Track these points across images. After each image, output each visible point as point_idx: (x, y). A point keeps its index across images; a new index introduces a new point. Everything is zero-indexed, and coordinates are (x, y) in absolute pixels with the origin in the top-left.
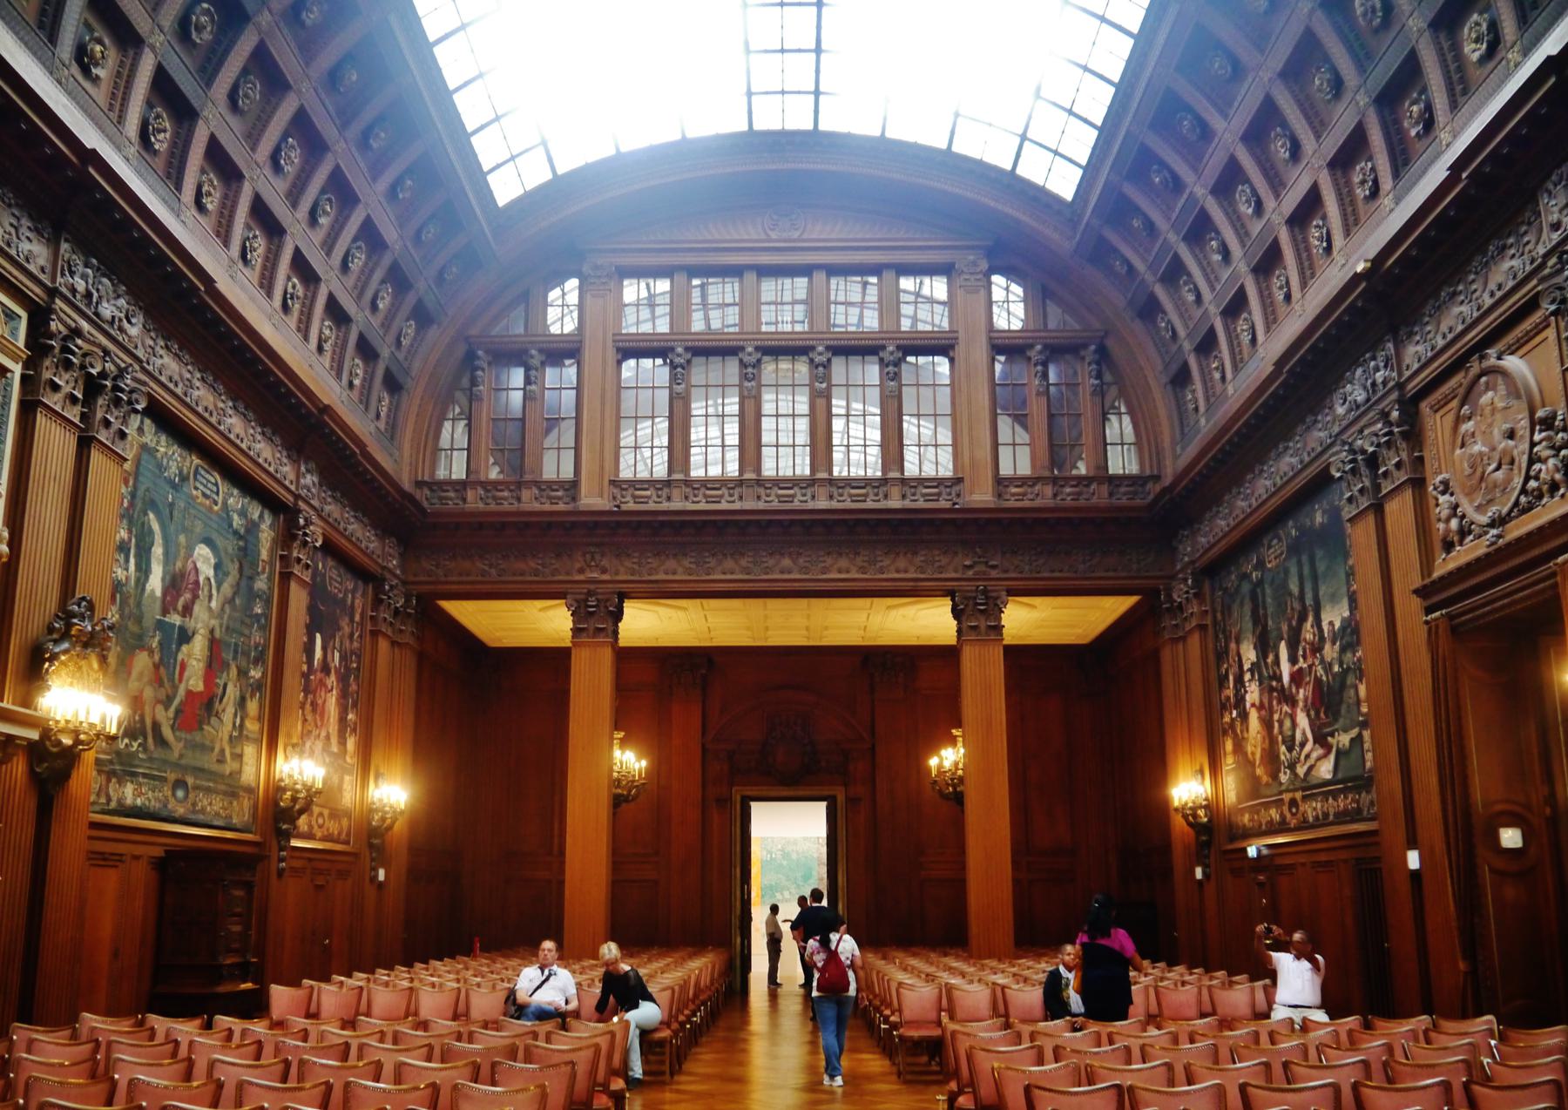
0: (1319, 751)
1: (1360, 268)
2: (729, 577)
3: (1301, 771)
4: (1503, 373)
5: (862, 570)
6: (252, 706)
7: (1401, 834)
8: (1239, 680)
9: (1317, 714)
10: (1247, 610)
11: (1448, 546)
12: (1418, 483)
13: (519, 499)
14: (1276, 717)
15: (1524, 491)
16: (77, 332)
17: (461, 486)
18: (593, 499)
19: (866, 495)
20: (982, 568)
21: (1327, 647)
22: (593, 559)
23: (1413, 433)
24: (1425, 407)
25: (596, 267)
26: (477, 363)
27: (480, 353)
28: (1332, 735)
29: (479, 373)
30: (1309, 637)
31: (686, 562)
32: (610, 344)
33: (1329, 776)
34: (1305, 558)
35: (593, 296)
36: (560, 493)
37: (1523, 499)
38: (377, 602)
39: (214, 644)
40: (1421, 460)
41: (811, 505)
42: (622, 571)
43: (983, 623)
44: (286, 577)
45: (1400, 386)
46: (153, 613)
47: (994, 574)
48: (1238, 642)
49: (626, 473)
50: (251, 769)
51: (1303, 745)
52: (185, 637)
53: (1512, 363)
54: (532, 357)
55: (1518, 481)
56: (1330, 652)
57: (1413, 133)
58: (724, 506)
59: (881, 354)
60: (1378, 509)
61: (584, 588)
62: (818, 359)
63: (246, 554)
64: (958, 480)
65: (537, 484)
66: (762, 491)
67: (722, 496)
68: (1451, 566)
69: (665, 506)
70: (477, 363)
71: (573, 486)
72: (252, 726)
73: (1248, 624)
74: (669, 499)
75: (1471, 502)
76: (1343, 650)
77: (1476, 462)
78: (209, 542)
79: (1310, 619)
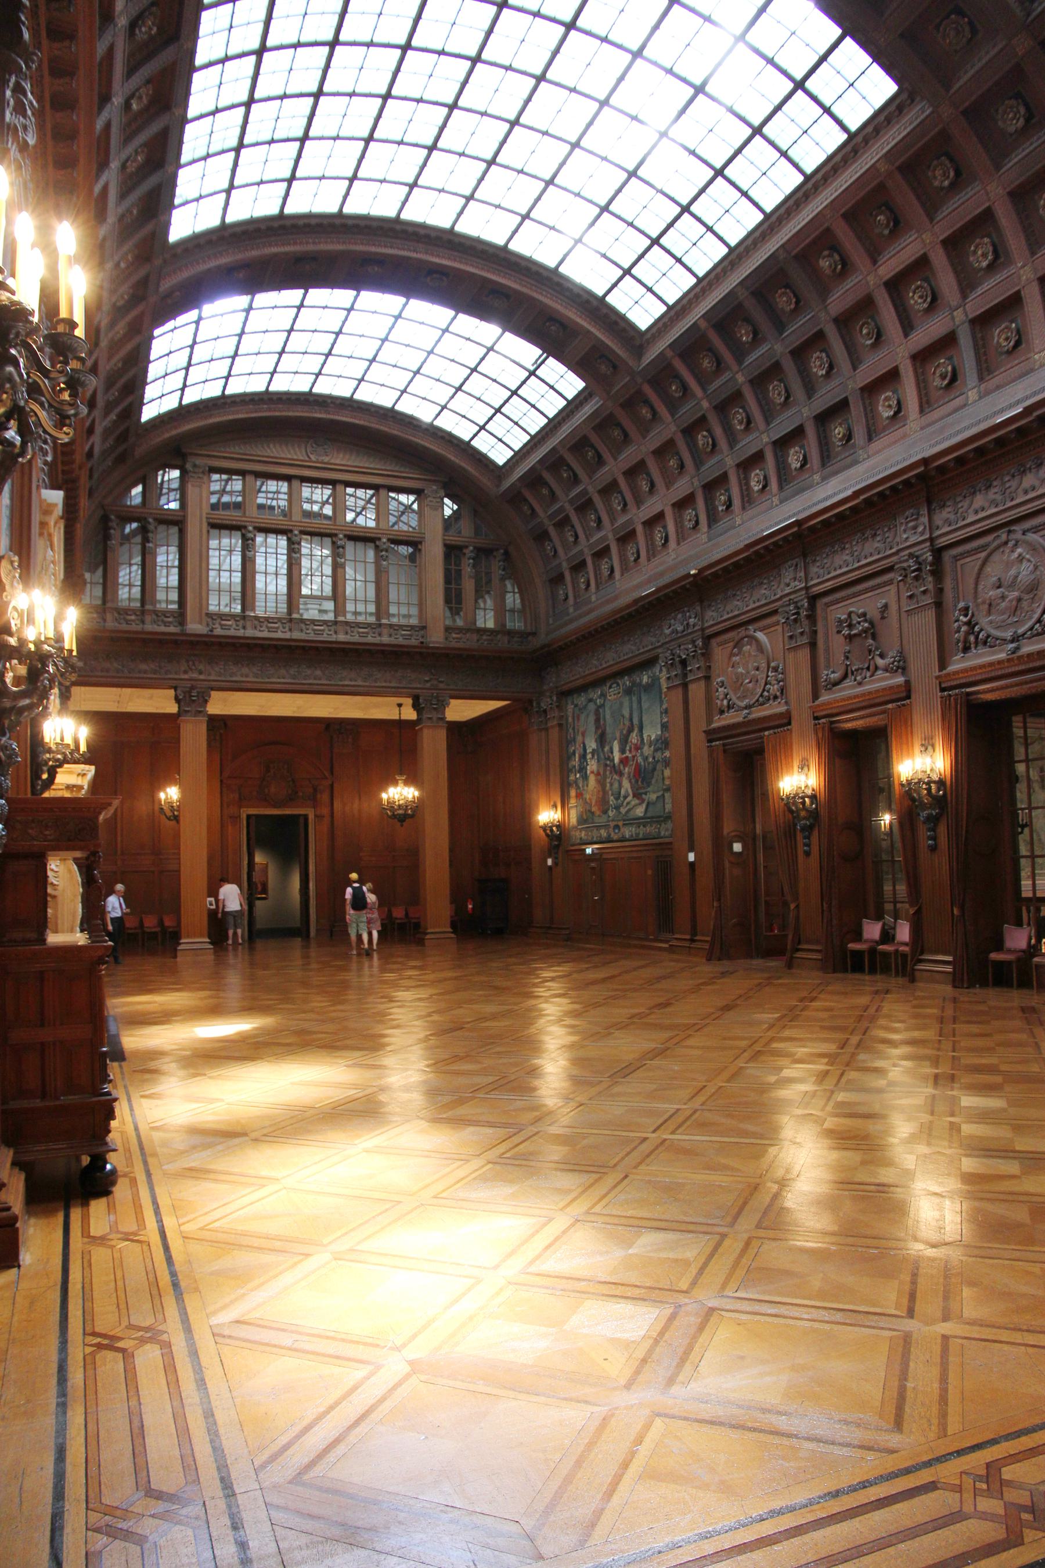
0: (636, 801)
1: (692, 572)
2: (282, 680)
3: (623, 810)
4: (757, 640)
5: (365, 679)
7: (686, 844)
8: (583, 756)
9: (637, 782)
10: (592, 719)
11: (722, 712)
12: (707, 678)
13: (143, 622)
14: (608, 780)
15: (761, 695)
18: (195, 627)
19: (367, 633)
20: (435, 682)
21: (646, 748)
22: (194, 664)
23: (707, 654)
24: (714, 642)
25: (195, 466)
26: (110, 524)
27: (113, 517)
28: (646, 794)
29: (112, 531)
30: (634, 741)
31: (255, 670)
32: (204, 520)
33: (641, 815)
34: (634, 698)
35: (193, 486)
36: (170, 619)
37: (761, 699)
40: (710, 667)
41: (333, 638)
42: (214, 673)
43: (435, 715)
45: (703, 630)
47: (441, 686)
48: (583, 735)
49: (213, 608)
51: (625, 797)
53: (759, 635)
54: (149, 523)
55: (759, 691)
56: (647, 751)
57: (720, 509)
58: (279, 635)
59: (378, 543)
60: (685, 686)
61: (188, 684)
62: (339, 543)
64: (424, 628)
65: (156, 612)
66: (303, 626)
67: (278, 628)
68: (723, 723)
69: (241, 633)
70: (110, 524)
71: (181, 615)
73: (592, 727)
74: (244, 628)
75: (735, 694)
76: (656, 750)
77: (739, 677)
79: (636, 731)
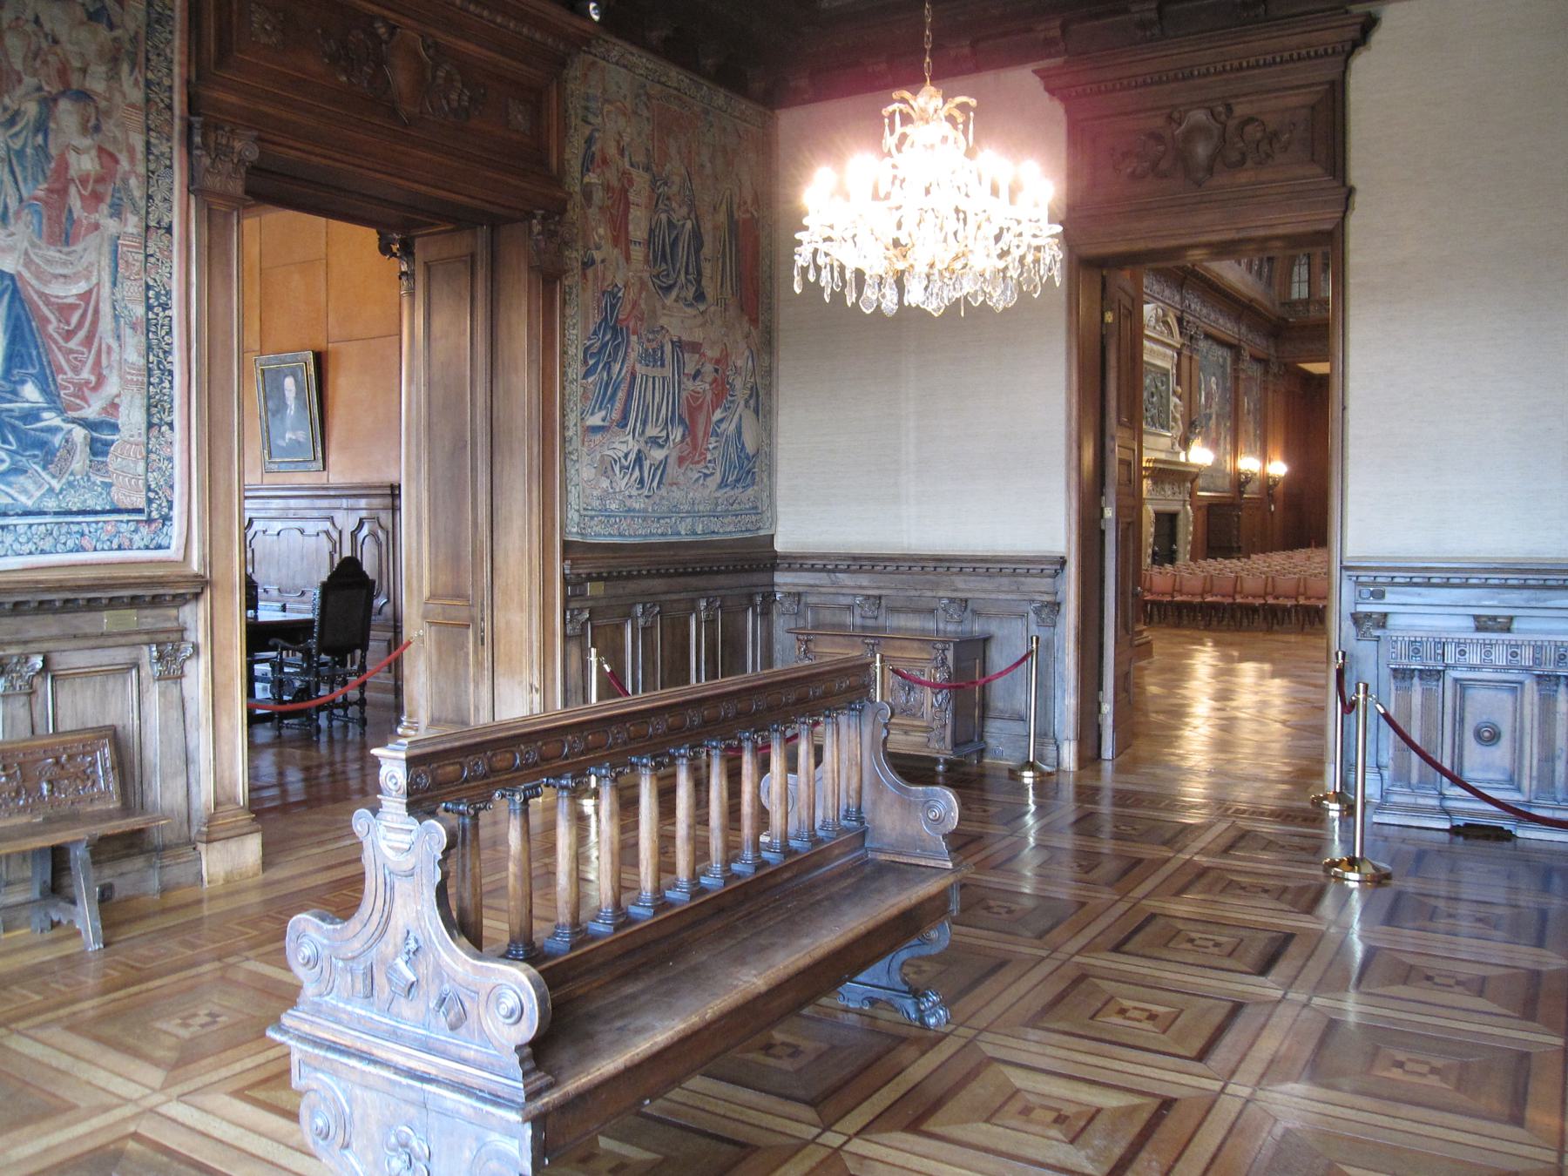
6: (1228, 438)
16: (1188, 322)
17: (1307, 302)
38: (1266, 372)
39: (1218, 416)
44: (1237, 378)
46: (1203, 412)
50: (1229, 466)
52: (1210, 418)
63: (1224, 372)
72: (1228, 447)
78: (1214, 375)
